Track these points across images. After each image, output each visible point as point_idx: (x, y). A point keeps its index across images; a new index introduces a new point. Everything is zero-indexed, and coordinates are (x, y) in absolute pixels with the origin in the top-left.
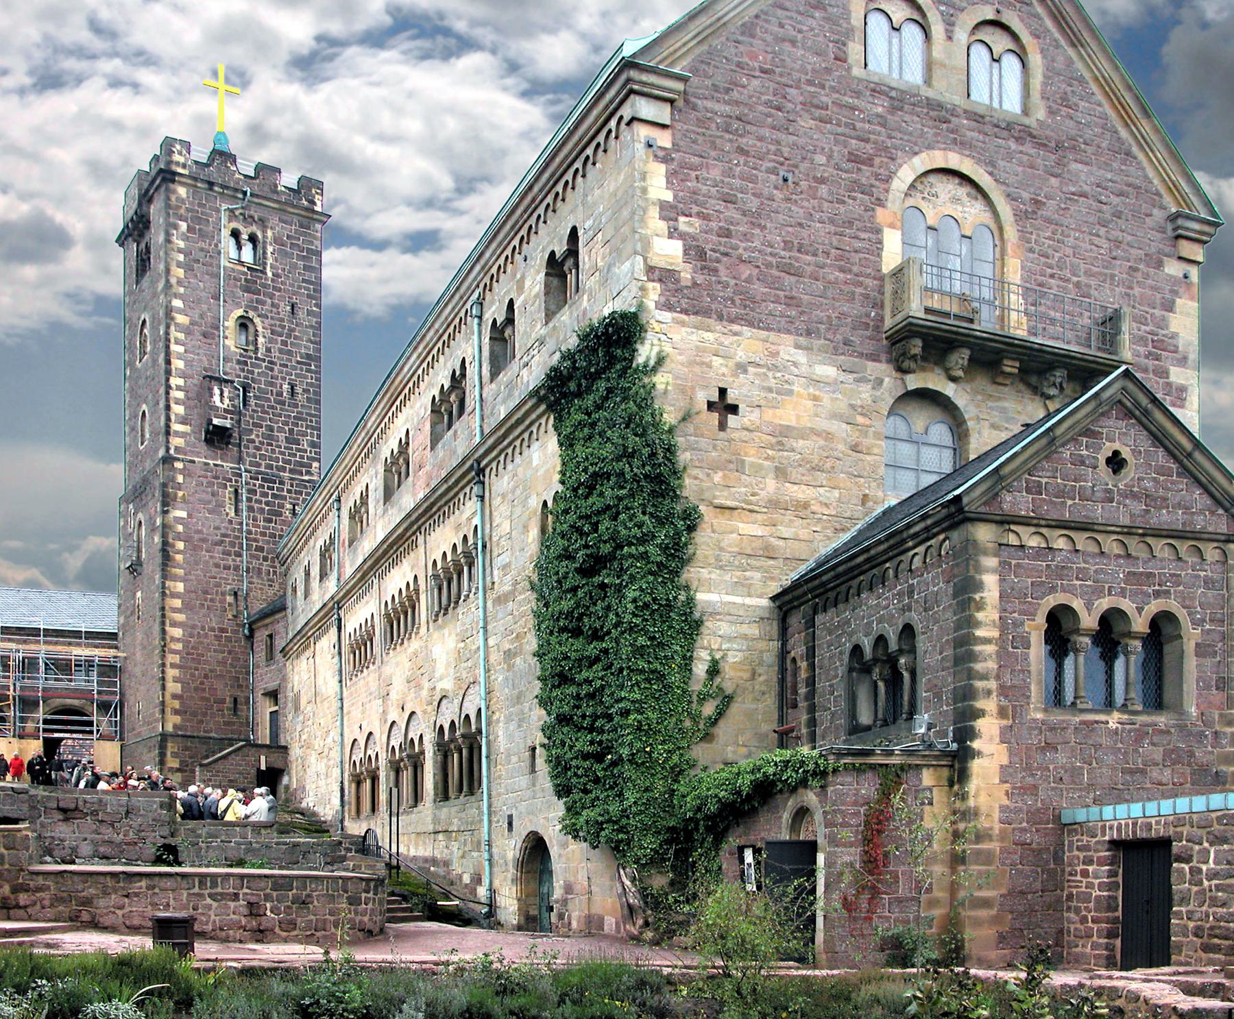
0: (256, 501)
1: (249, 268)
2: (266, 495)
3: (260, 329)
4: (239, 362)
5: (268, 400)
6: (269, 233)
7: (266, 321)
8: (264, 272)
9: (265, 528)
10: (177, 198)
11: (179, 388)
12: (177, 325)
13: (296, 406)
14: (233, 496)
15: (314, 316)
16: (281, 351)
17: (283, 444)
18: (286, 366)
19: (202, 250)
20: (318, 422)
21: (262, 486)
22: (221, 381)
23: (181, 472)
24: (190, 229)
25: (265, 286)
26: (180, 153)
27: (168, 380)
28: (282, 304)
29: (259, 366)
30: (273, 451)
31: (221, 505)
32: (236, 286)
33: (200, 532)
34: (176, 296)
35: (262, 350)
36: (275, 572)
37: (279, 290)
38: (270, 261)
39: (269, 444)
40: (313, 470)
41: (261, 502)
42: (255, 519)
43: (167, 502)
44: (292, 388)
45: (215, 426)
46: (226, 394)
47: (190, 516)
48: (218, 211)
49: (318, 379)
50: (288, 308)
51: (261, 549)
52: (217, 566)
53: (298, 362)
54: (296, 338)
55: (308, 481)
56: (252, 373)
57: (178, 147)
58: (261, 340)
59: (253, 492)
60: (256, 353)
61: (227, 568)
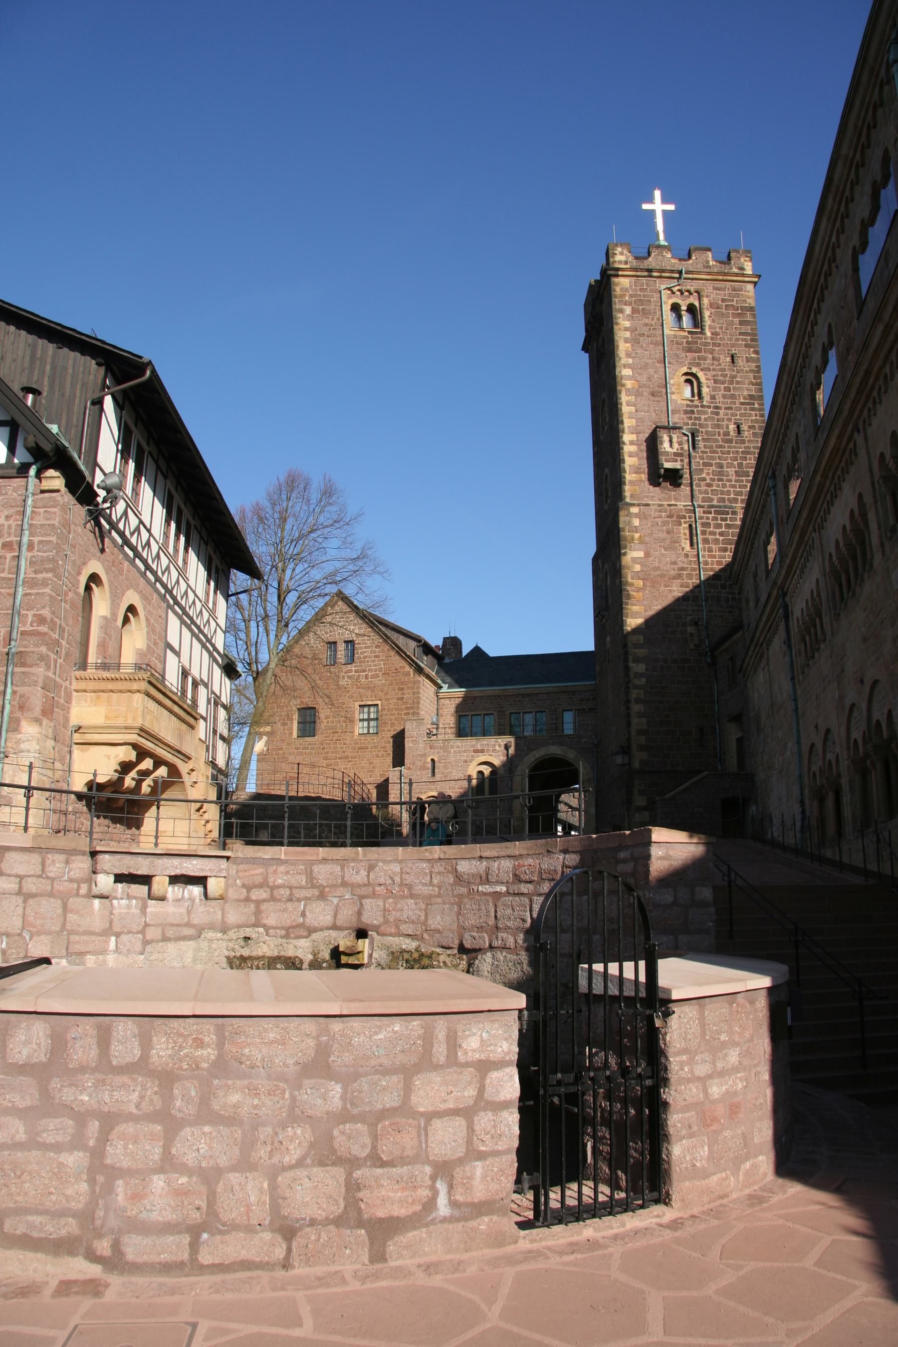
0: (711, 533)
1: (689, 332)
2: (720, 526)
3: (702, 379)
4: (686, 412)
5: (717, 441)
6: (705, 301)
7: (708, 373)
9: (721, 557)
12: (628, 390)
13: (743, 442)
14: (687, 532)
15: (753, 362)
16: (724, 397)
17: (734, 478)
18: (731, 408)
19: (646, 325)
21: (715, 519)
22: (669, 428)
24: (634, 311)
25: (706, 344)
26: (622, 254)
28: (722, 357)
29: (705, 413)
30: (724, 486)
32: (678, 349)
37: (719, 345)
39: (719, 480)
41: (714, 534)
42: (710, 550)
44: (738, 427)
45: (667, 470)
46: (675, 440)
50: (729, 359)
53: (742, 404)
54: (738, 383)
56: (699, 419)
58: (705, 390)
59: (707, 525)
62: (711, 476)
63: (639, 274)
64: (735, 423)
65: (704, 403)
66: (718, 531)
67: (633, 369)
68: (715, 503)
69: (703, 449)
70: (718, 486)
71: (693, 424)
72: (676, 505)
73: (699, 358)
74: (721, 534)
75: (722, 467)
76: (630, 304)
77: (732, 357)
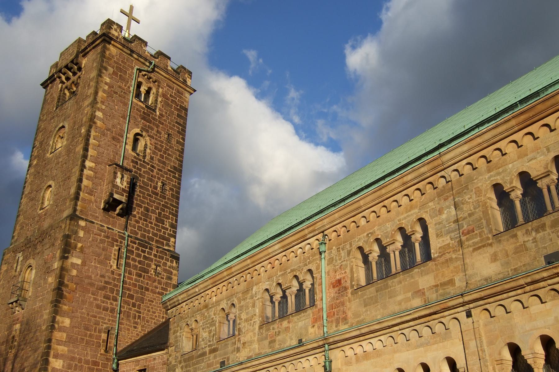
4: (133, 161)
5: (148, 190)
7: (153, 140)
8: (154, 110)
9: (136, 280)
10: (110, 54)
11: (91, 169)
14: (117, 253)
16: (159, 161)
17: (154, 222)
18: (161, 171)
19: (120, 87)
20: (177, 212)
21: (137, 249)
23: (83, 228)
25: (154, 119)
26: (116, 30)
27: (84, 161)
28: (163, 133)
29: (145, 167)
31: (108, 258)
33: (90, 277)
34: (99, 109)
35: (147, 158)
36: (139, 317)
38: (159, 105)
40: (171, 243)
42: (130, 273)
43: (67, 250)
47: (84, 263)
48: (133, 68)
49: (179, 184)
50: (166, 136)
51: (131, 297)
52: (98, 307)
53: (169, 170)
54: (169, 155)
55: (168, 250)
56: (140, 170)
57: (115, 27)
60: (145, 158)
61: (106, 309)
62: (140, 215)
63: (125, 50)
64: (162, 182)
65: (146, 160)
66: (138, 259)
67: (103, 114)
68: (139, 236)
69: (138, 193)
70: (143, 224)
71: (136, 172)
72: (113, 230)
73: (149, 127)
74: (140, 262)
75: (148, 211)
76: (113, 67)
77: (169, 135)
